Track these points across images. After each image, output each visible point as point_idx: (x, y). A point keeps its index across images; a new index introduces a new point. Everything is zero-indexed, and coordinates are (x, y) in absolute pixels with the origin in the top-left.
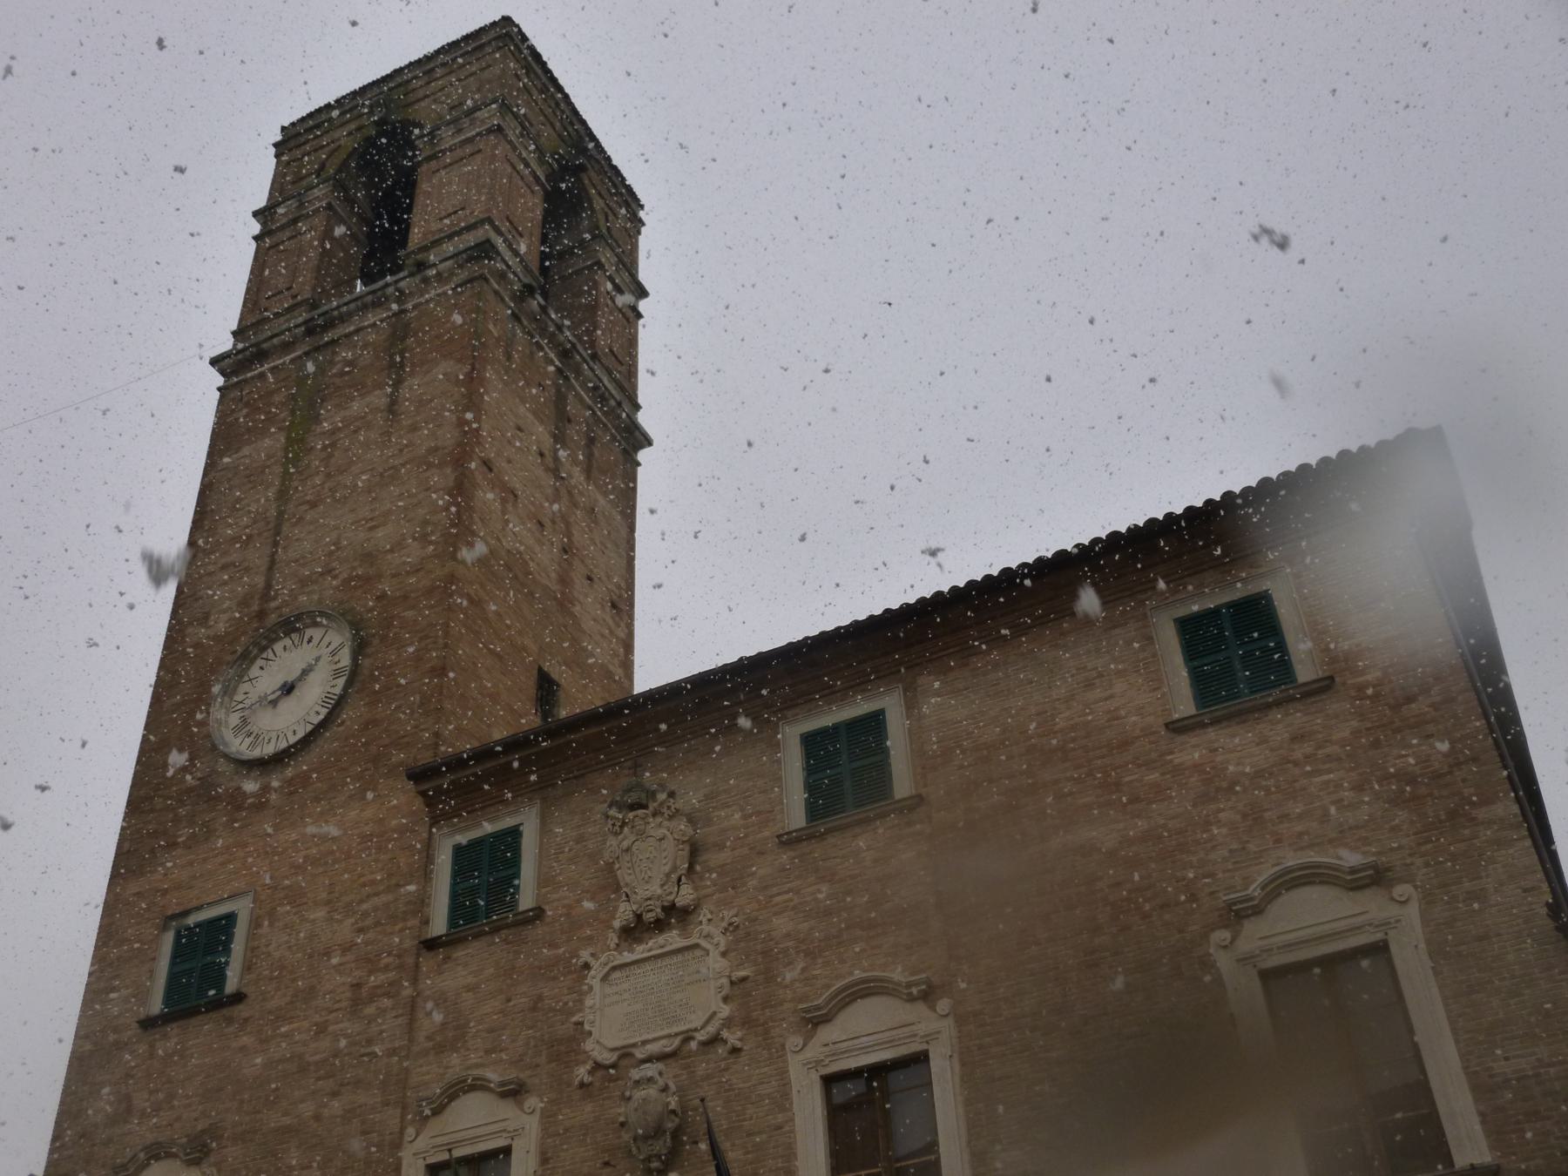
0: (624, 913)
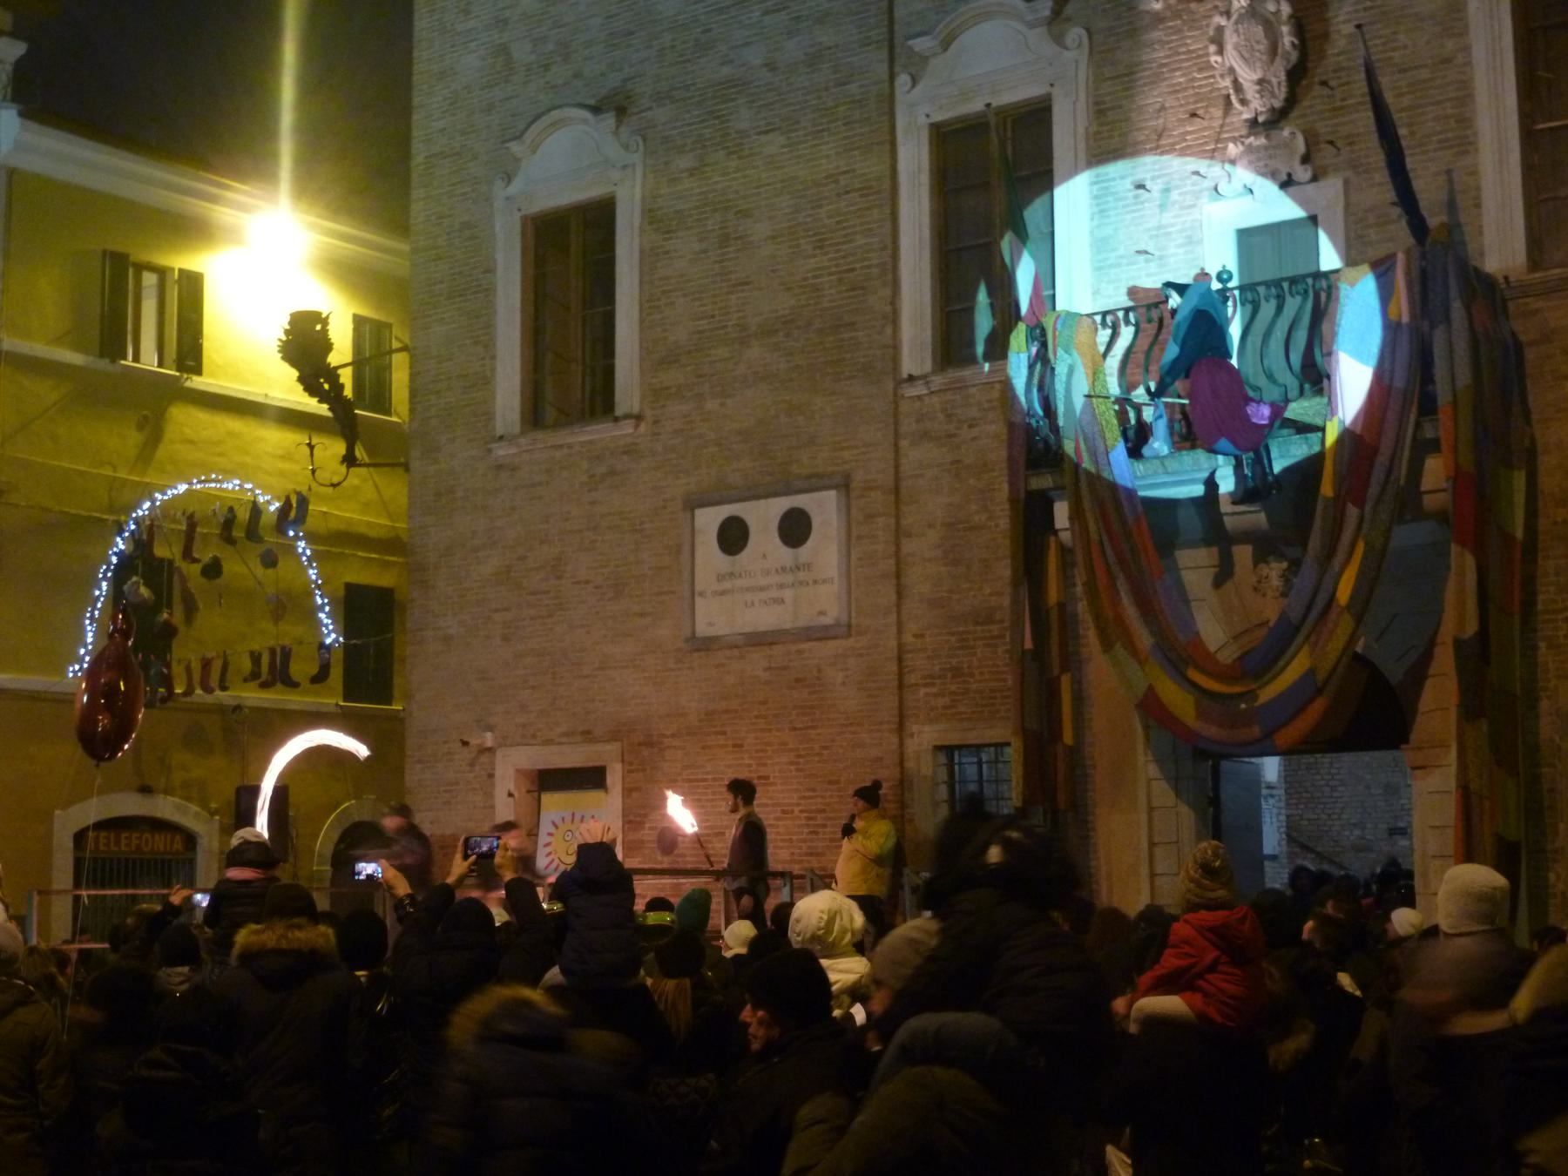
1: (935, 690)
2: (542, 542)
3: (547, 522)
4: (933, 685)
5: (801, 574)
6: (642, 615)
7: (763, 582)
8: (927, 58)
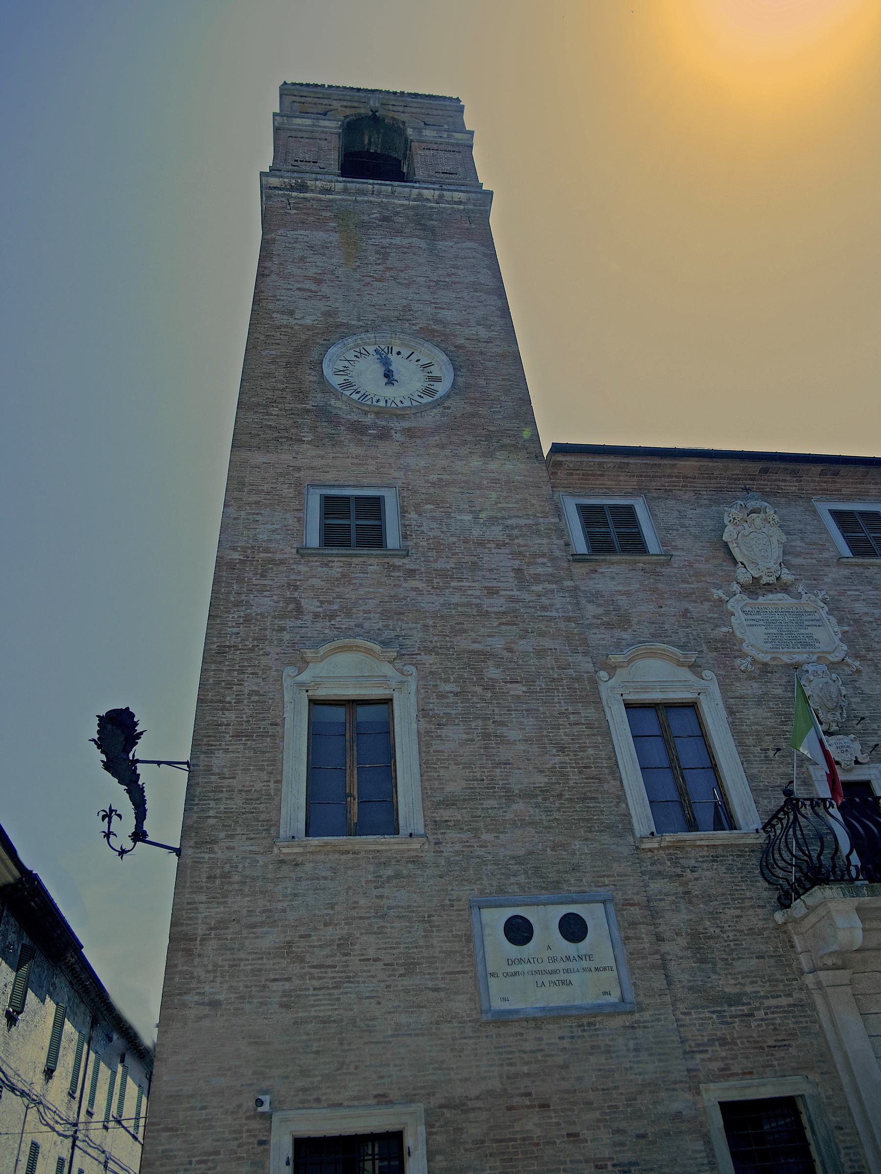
0: (743, 575)
1: (708, 1056)
2: (326, 925)
3: (332, 908)
4: (707, 1051)
5: (584, 962)
6: (436, 990)
7: (551, 967)
8: (615, 667)
